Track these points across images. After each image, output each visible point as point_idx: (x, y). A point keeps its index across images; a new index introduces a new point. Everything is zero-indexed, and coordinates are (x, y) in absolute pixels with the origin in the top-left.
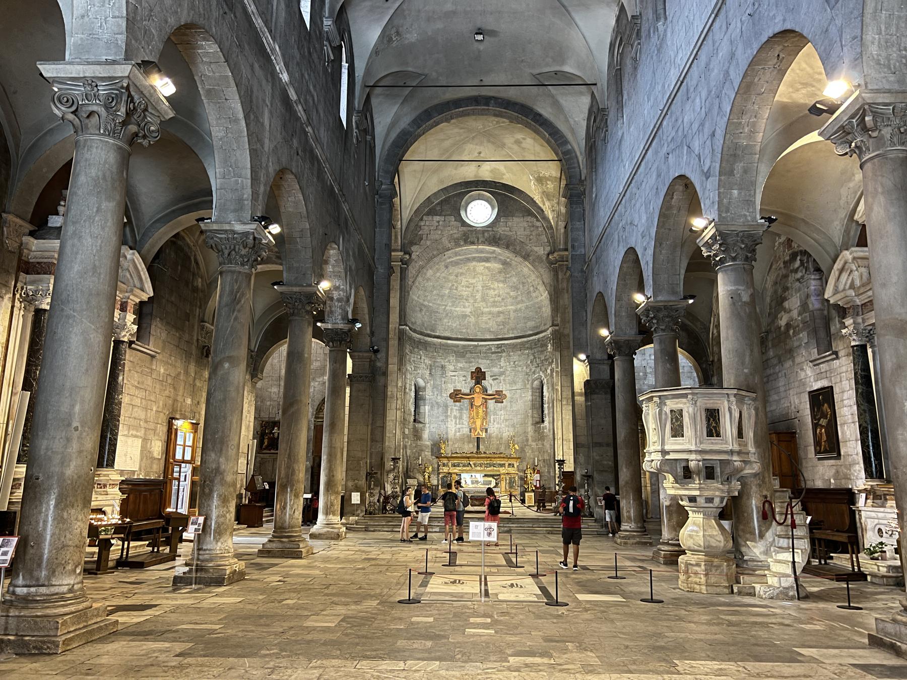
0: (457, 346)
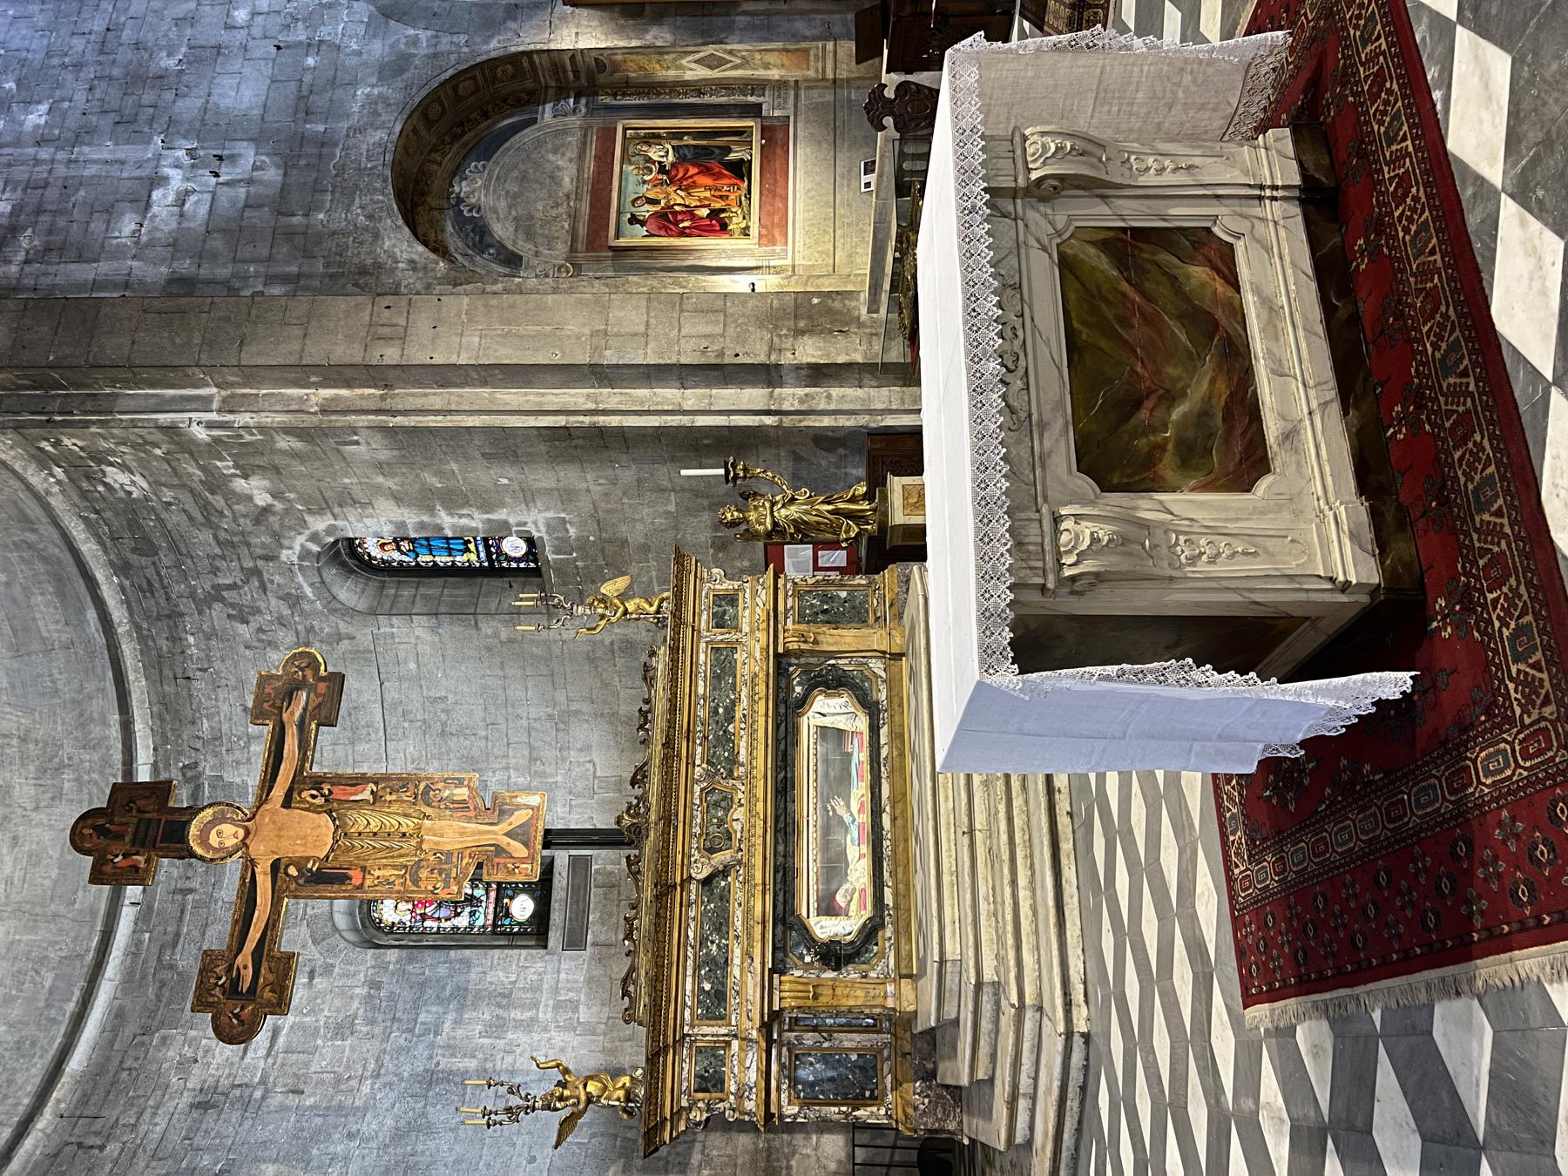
0: (118, 1016)
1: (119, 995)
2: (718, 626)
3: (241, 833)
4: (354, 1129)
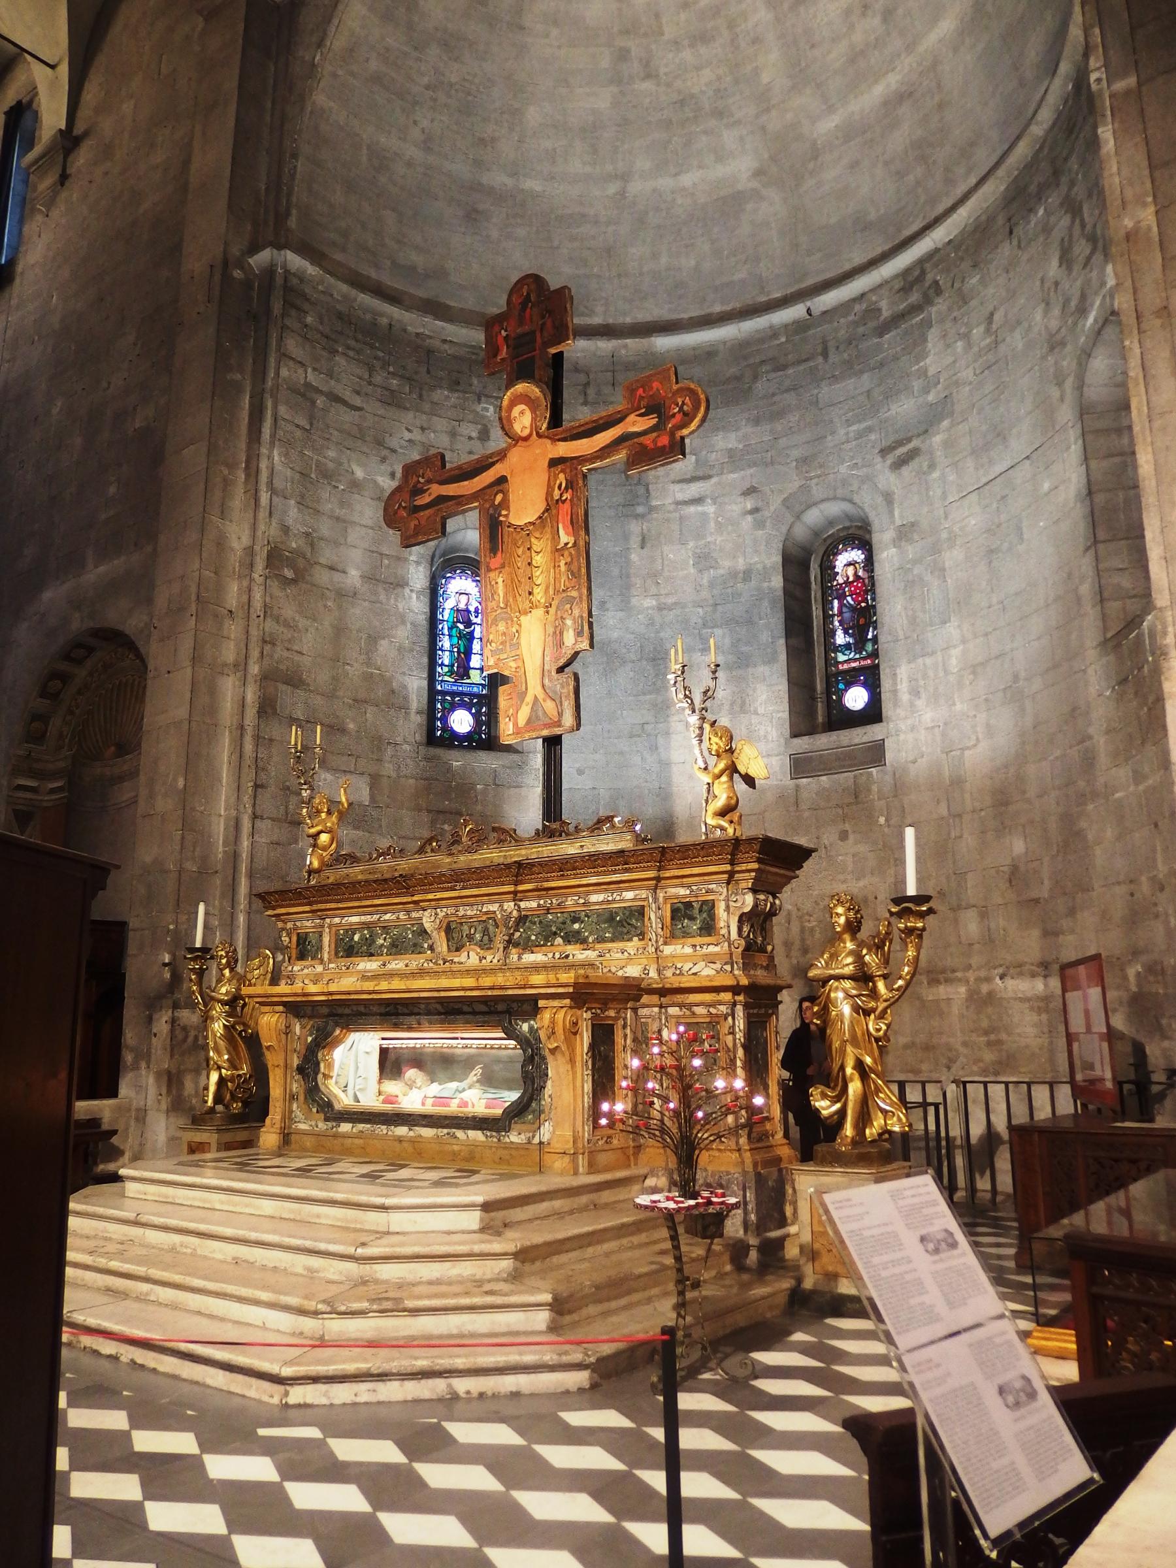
0: (708, 354)
1: (728, 344)
2: (675, 912)
3: (526, 432)
4: (608, 605)
